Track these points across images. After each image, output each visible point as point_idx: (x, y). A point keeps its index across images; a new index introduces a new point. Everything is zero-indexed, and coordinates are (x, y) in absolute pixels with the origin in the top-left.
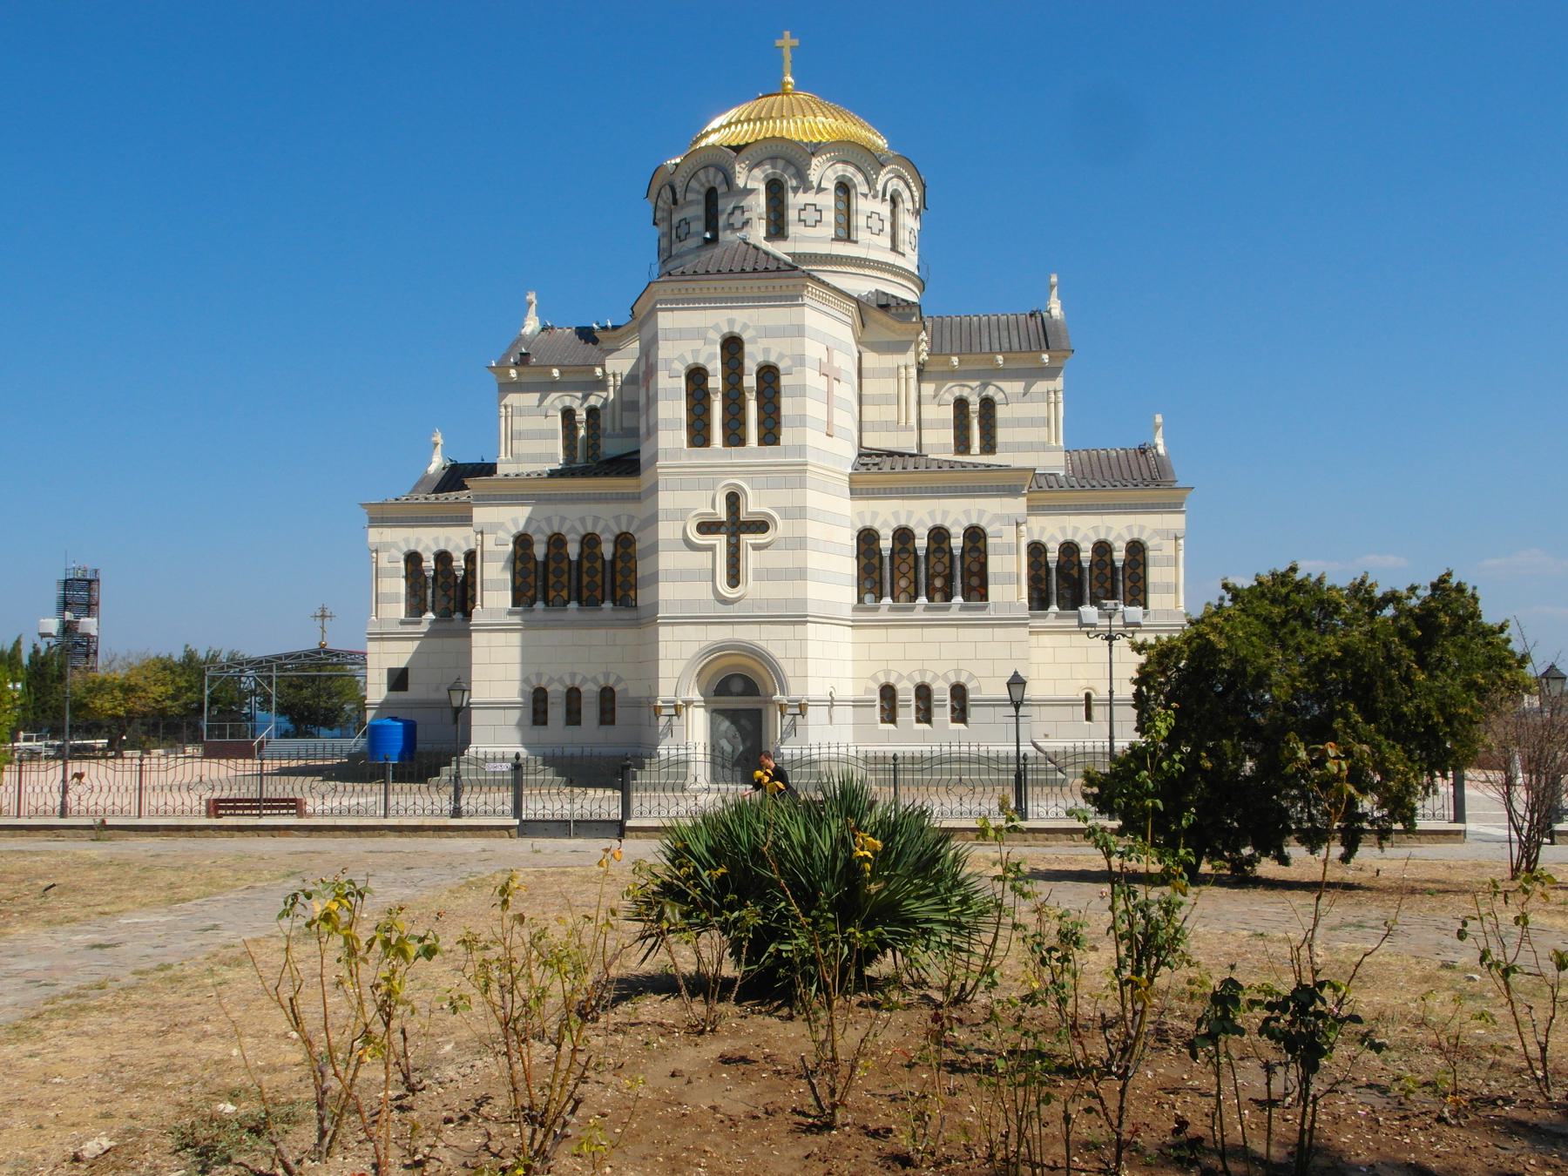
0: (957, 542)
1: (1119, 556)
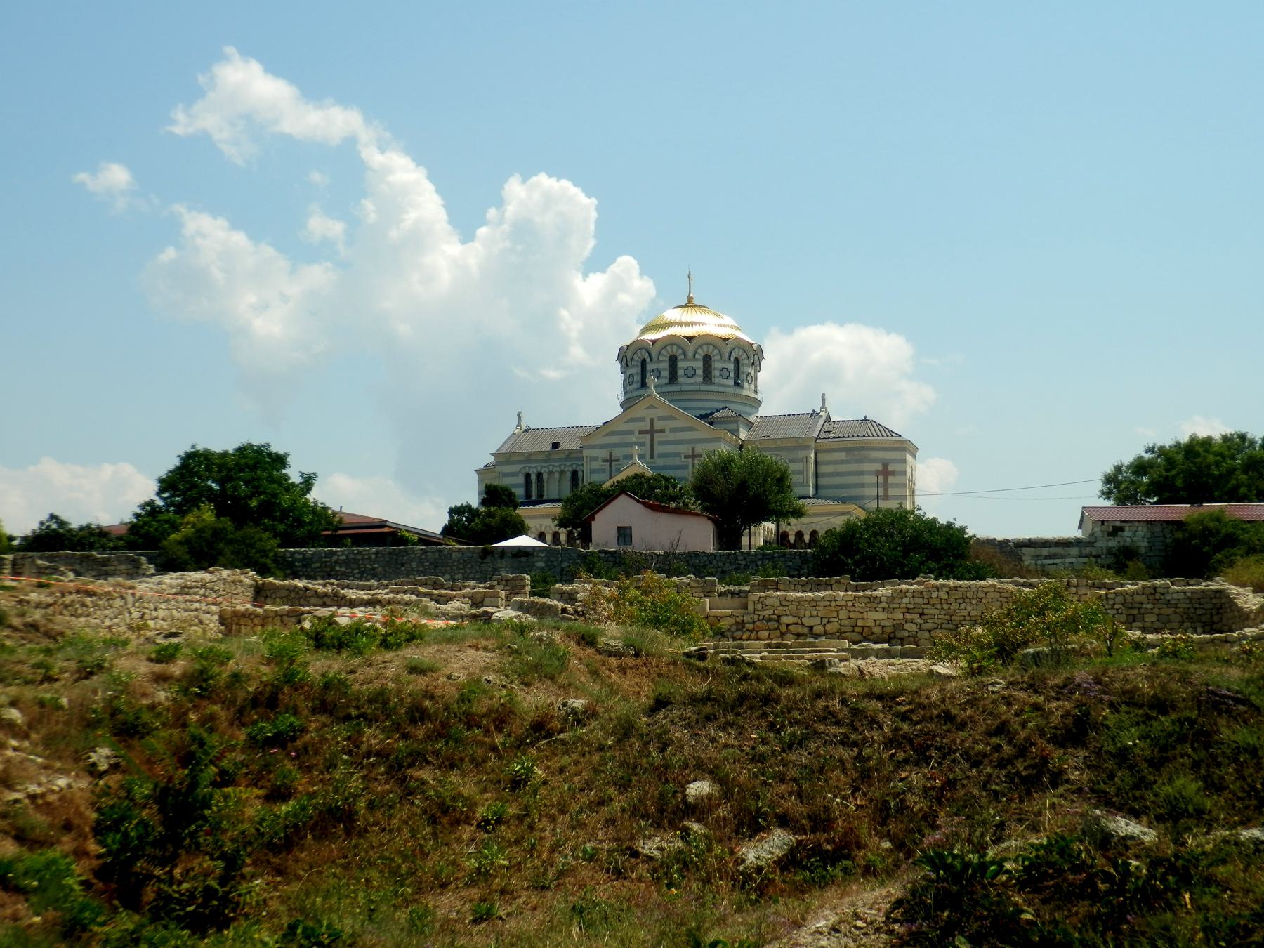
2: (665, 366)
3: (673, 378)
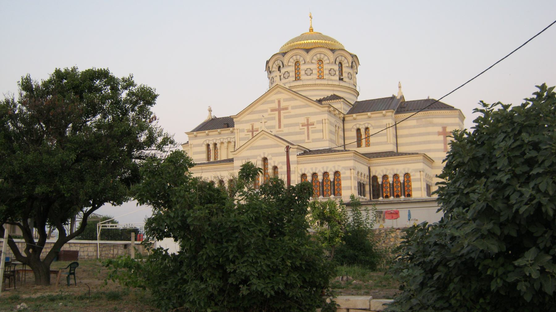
0: (331, 177)
1: (401, 179)
2: (291, 69)
3: (297, 78)
